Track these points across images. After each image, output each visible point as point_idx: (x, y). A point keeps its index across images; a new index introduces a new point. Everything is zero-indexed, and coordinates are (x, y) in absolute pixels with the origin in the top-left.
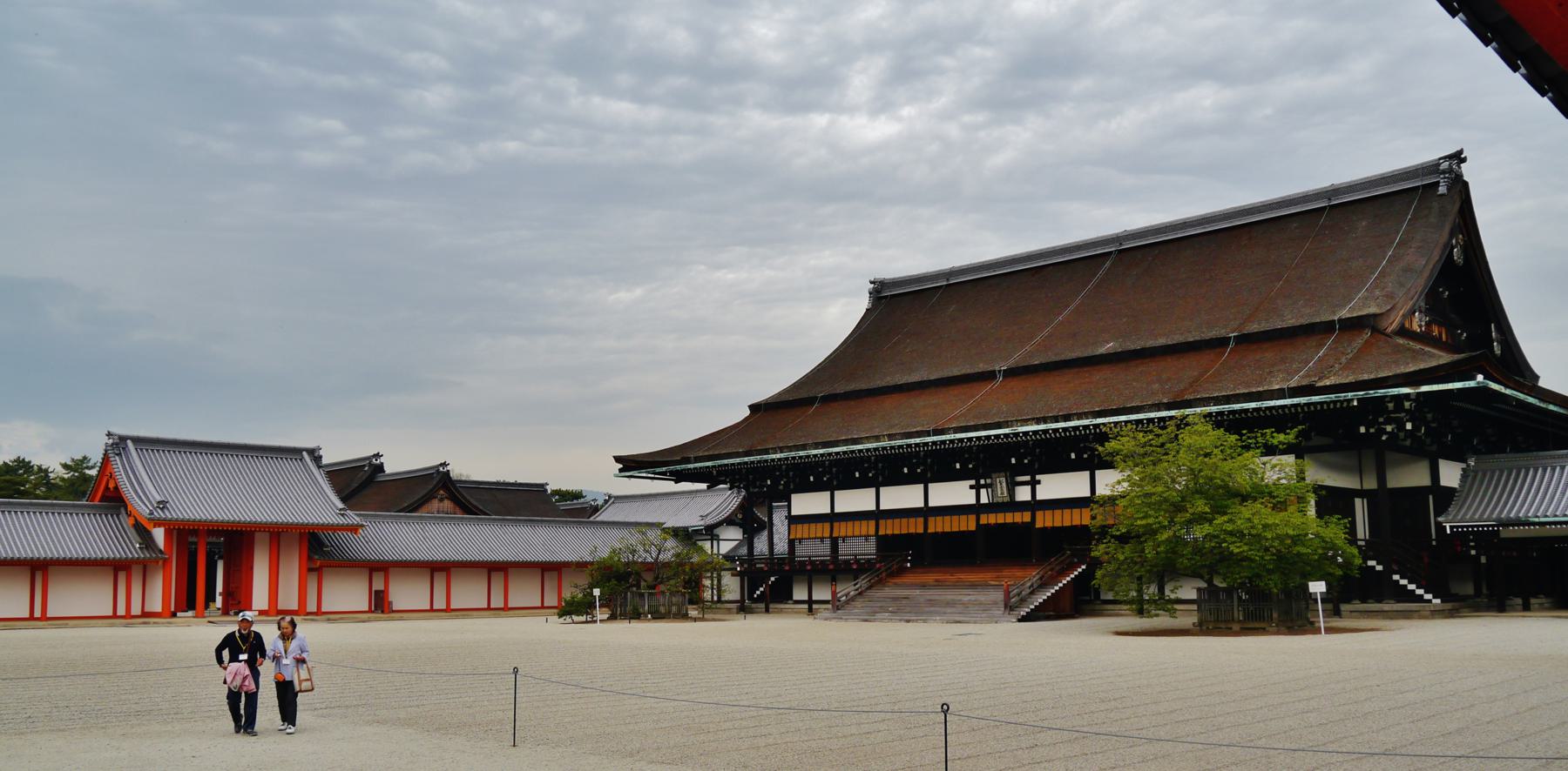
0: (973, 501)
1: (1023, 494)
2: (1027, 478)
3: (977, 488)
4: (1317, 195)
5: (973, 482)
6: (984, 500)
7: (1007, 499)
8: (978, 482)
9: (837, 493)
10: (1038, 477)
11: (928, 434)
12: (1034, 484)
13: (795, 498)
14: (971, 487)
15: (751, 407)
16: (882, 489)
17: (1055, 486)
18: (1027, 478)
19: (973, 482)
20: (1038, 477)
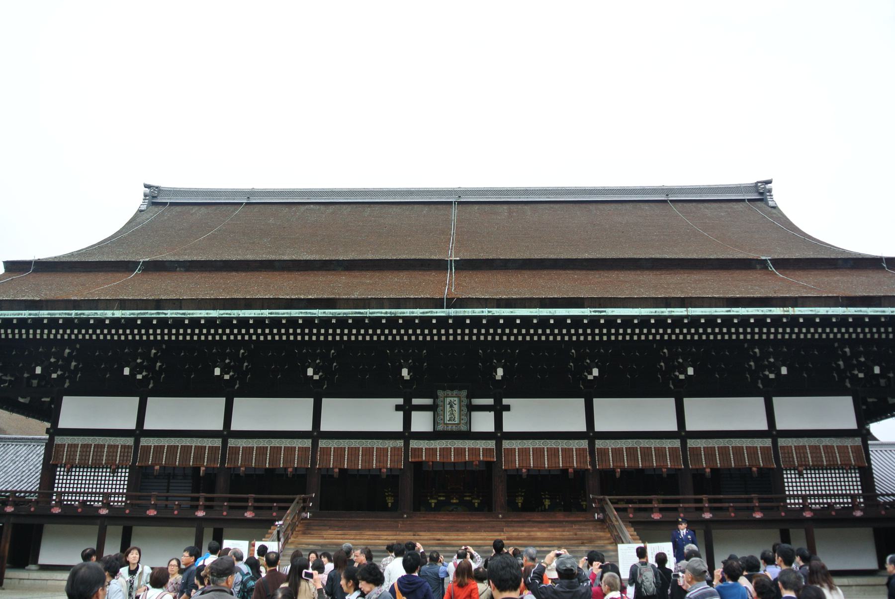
0: (400, 428)
1: (483, 422)
2: (490, 401)
3: (407, 410)
4: (654, 191)
5: (400, 401)
6: (422, 422)
7: (464, 428)
8: (408, 401)
9: (151, 401)
10: (506, 401)
11: (438, 303)
12: (499, 410)
13: (66, 400)
14: (398, 408)
15: (4, 262)
16: (237, 401)
17: (527, 415)
18: (490, 401)
19: (400, 401)
20: (506, 401)
